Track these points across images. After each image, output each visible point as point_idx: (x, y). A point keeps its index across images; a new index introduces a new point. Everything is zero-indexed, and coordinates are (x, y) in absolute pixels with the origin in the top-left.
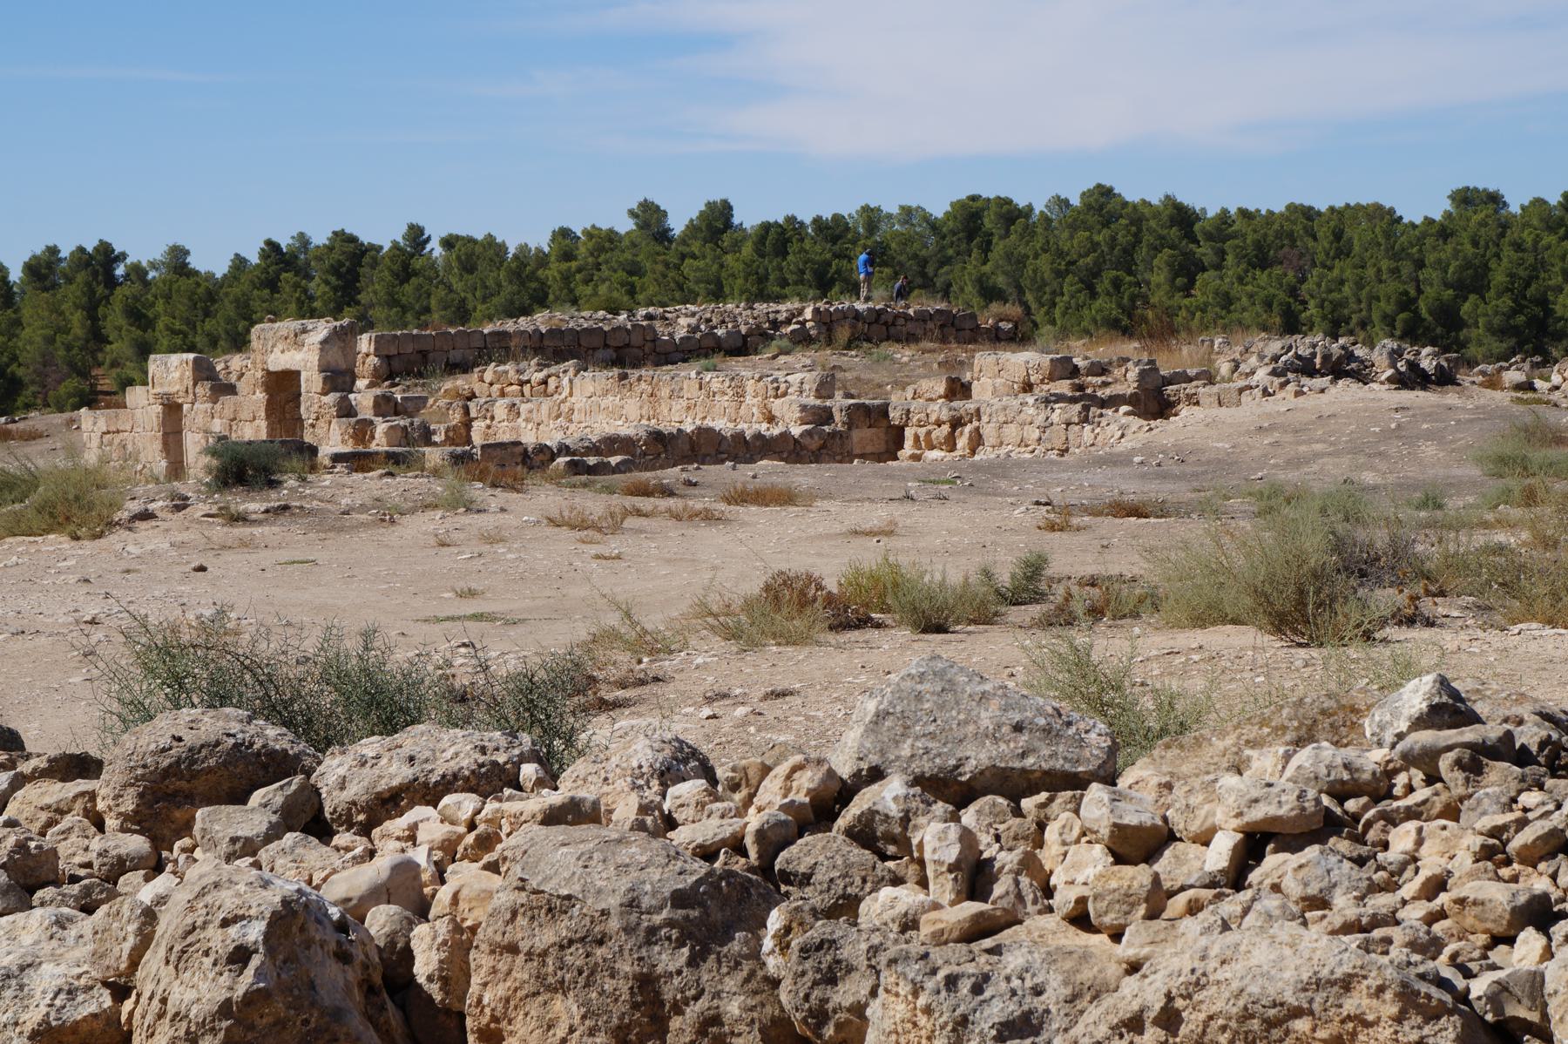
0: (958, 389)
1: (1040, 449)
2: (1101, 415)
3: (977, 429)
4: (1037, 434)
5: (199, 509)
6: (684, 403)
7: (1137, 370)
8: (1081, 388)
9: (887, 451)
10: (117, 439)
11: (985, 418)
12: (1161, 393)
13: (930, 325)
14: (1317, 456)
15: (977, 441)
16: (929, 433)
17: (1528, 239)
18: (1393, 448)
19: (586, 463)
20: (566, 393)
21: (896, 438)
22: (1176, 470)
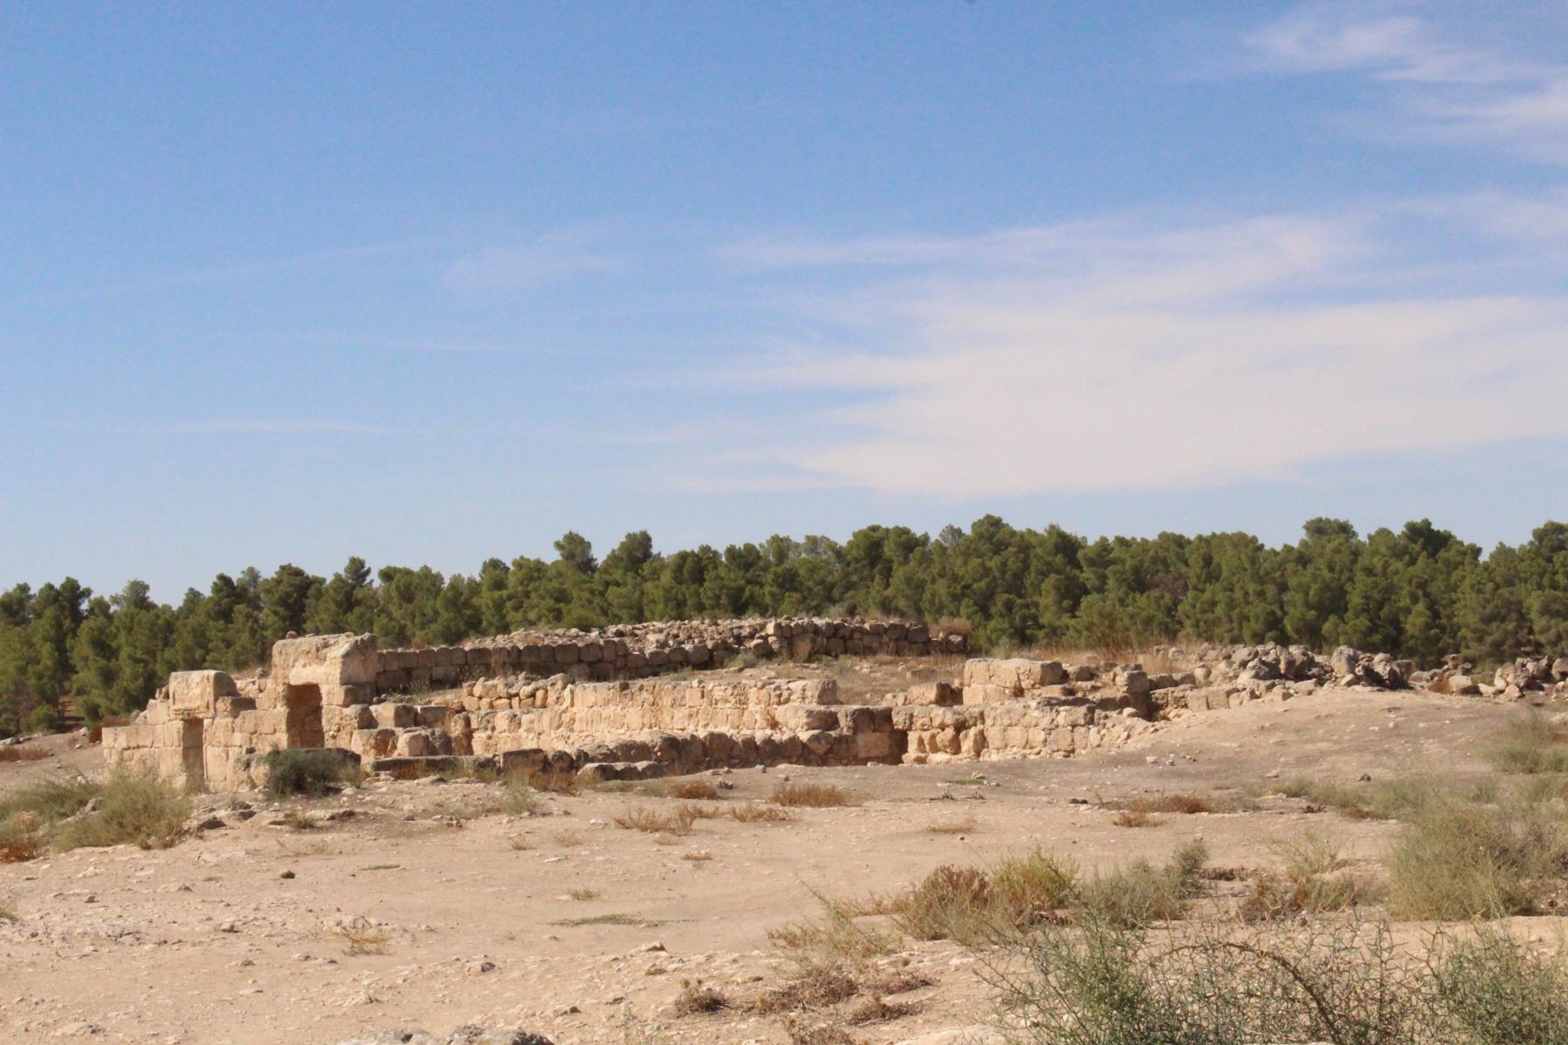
0: (949, 696)
1: (1045, 751)
2: (1106, 717)
3: (982, 732)
4: (1042, 736)
5: (265, 817)
6: (686, 711)
7: (1126, 674)
8: (1071, 692)
9: (891, 755)
10: (137, 754)
11: (989, 722)
12: (1149, 697)
13: (885, 639)
14: (1323, 754)
15: (981, 743)
16: (933, 737)
17: (1378, 563)
18: (1396, 746)
19: (618, 767)
20: (567, 703)
21: (899, 742)
22: (1191, 769)
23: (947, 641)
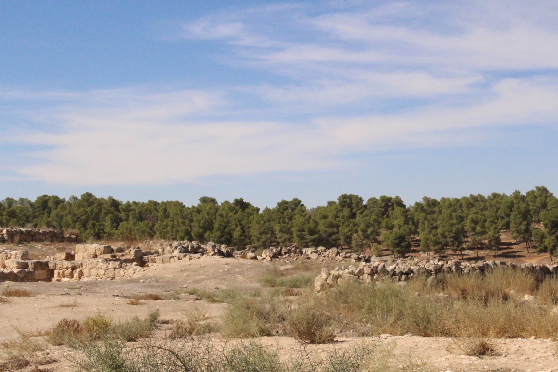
0: (70, 257)
1: (104, 278)
2: (126, 266)
3: (81, 270)
4: (103, 272)
7: (134, 250)
8: (114, 256)
9: (48, 278)
11: (84, 267)
12: (142, 258)
13: (47, 236)
14: (203, 280)
15: (81, 274)
16: (63, 272)
17: (224, 213)
18: (228, 277)
21: (51, 273)
22: (156, 284)
23: (70, 237)
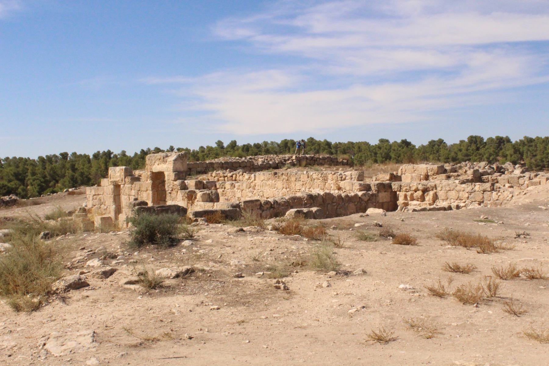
3: (436, 193)
4: (467, 195)
5: (125, 273)
6: (302, 183)
10: (98, 197)
11: (439, 189)
13: (326, 161)
15: (436, 198)
16: (412, 195)
20: (253, 179)
23: (342, 162)
